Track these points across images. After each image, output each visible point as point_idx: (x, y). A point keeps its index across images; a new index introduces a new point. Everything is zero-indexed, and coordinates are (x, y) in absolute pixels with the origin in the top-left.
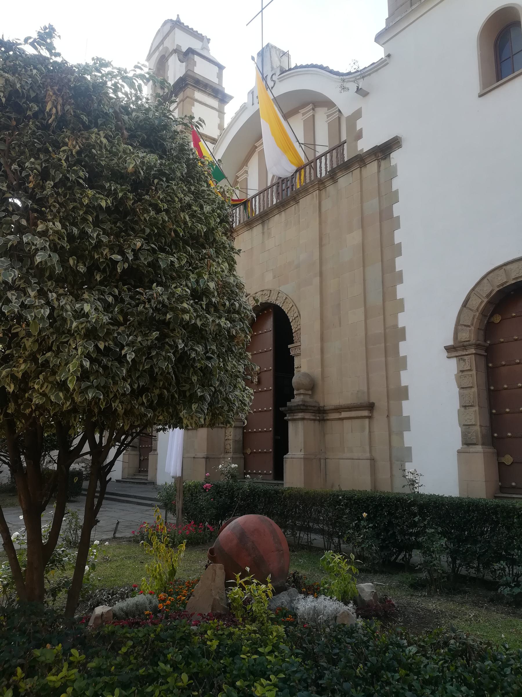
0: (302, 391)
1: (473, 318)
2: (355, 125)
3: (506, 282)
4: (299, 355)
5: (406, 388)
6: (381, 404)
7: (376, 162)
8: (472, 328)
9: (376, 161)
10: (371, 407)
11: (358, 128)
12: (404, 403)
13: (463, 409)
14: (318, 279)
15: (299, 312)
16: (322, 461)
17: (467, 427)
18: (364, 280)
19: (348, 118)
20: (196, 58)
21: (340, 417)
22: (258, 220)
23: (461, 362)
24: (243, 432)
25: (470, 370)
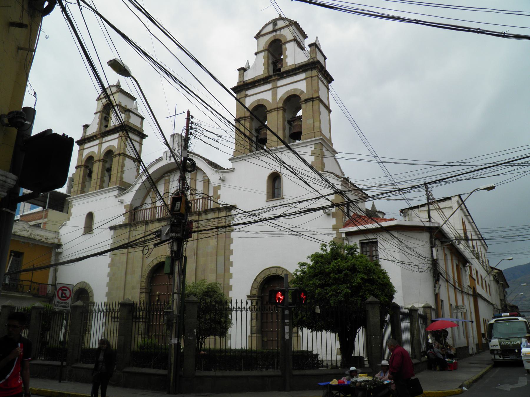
2: (217, 192)
7: (225, 212)
8: (257, 289)
11: (219, 194)
18: (217, 262)
19: (214, 187)
20: (131, 114)
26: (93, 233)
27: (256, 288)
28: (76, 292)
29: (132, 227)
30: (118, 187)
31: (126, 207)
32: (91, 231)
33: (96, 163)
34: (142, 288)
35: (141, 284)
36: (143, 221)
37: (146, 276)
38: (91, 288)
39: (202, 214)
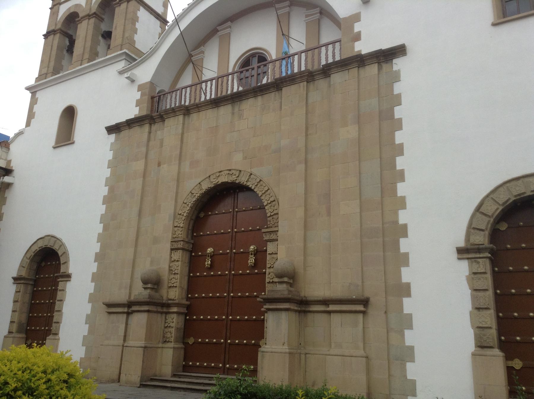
0: (286, 279)
1: (488, 223)
2: (352, 28)
3: (524, 193)
4: (277, 240)
5: (408, 285)
6: (378, 300)
7: (377, 64)
9: (377, 63)
10: (365, 302)
11: (356, 30)
12: (406, 300)
13: (476, 311)
14: (302, 167)
15: (275, 196)
16: (303, 356)
17: (481, 329)
21: (328, 309)
22: (228, 100)
23: (474, 264)
24: (186, 319)
25: (485, 273)
26: (73, 143)
27: (484, 228)
28: (35, 255)
29: (155, 123)
30: (125, 53)
31: (140, 88)
32: (70, 140)
33: (83, 22)
34: (176, 239)
35: (174, 233)
36: (179, 107)
37: (185, 214)
38: (65, 248)
39: (316, 77)
